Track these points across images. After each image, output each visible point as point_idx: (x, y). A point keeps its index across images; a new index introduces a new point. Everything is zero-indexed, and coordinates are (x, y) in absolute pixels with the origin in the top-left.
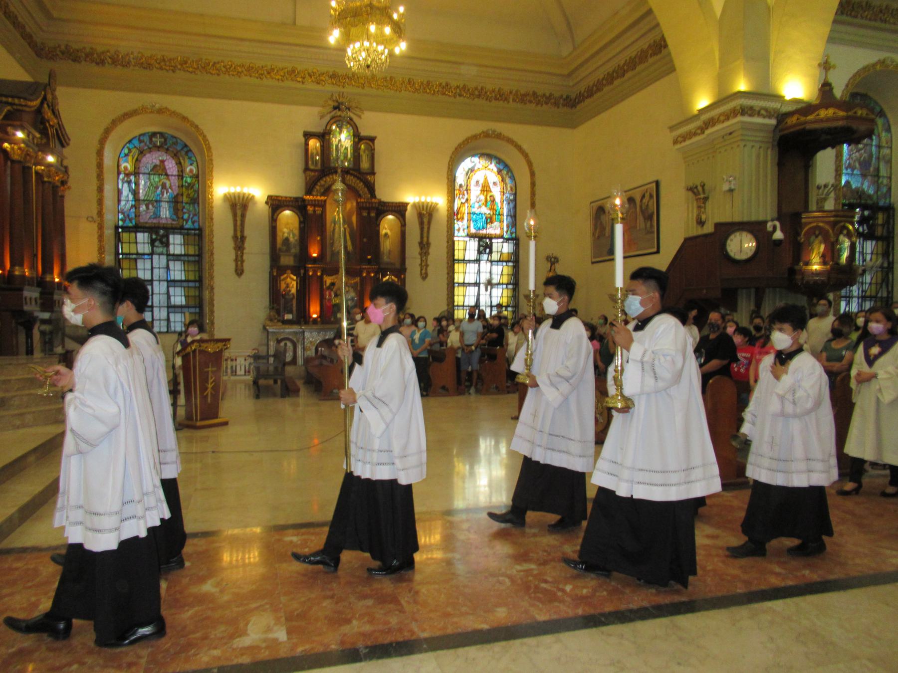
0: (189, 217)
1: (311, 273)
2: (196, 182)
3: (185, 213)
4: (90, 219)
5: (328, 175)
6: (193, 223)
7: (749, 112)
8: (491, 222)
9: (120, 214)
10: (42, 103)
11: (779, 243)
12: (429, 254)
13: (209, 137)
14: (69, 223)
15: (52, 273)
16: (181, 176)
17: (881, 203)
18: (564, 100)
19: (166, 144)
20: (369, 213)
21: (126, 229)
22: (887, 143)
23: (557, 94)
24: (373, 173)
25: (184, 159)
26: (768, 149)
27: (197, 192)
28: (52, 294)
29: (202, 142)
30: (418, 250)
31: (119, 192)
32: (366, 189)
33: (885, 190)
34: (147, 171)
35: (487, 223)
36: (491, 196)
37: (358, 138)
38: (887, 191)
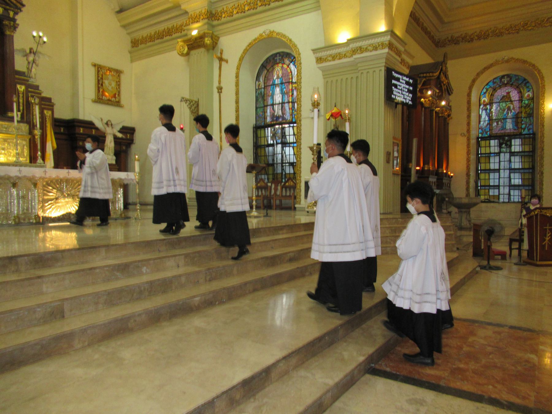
0: (526, 126)
2: (532, 103)
3: (523, 124)
4: (463, 135)
6: (529, 130)
9: (480, 130)
10: (440, 73)
14: (451, 137)
15: (442, 167)
16: (521, 100)
19: (511, 82)
21: (483, 139)
25: (523, 89)
27: (533, 109)
28: (442, 179)
29: (537, 75)
31: (480, 116)
34: (498, 101)
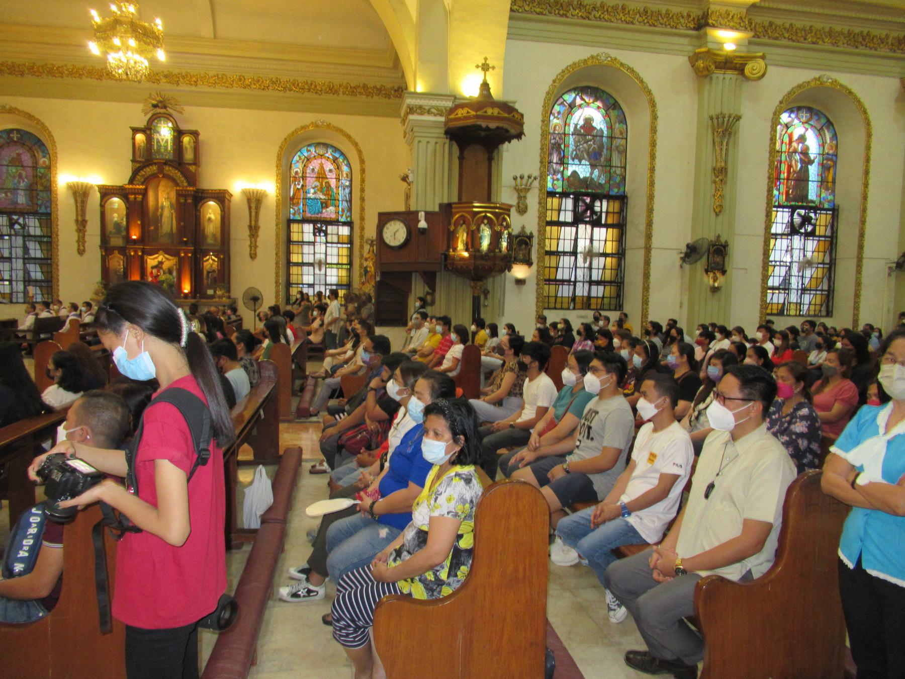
0: (42, 203)
1: (132, 254)
5: (148, 166)
7: (418, 111)
8: (327, 207)
11: (423, 231)
12: (257, 236)
13: (54, 133)
17: (615, 191)
18: (395, 91)
20: (186, 200)
22: (621, 133)
23: (389, 86)
24: (196, 162)
25: (38, 153)
26: (444, 144)
30: (248, 232)
32: (183, 179)
33: (618, 179)
35: (322, 207)
36: (326, 183)
37: (179, 133)
38: (621, 181)
